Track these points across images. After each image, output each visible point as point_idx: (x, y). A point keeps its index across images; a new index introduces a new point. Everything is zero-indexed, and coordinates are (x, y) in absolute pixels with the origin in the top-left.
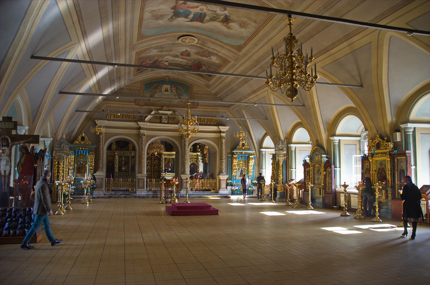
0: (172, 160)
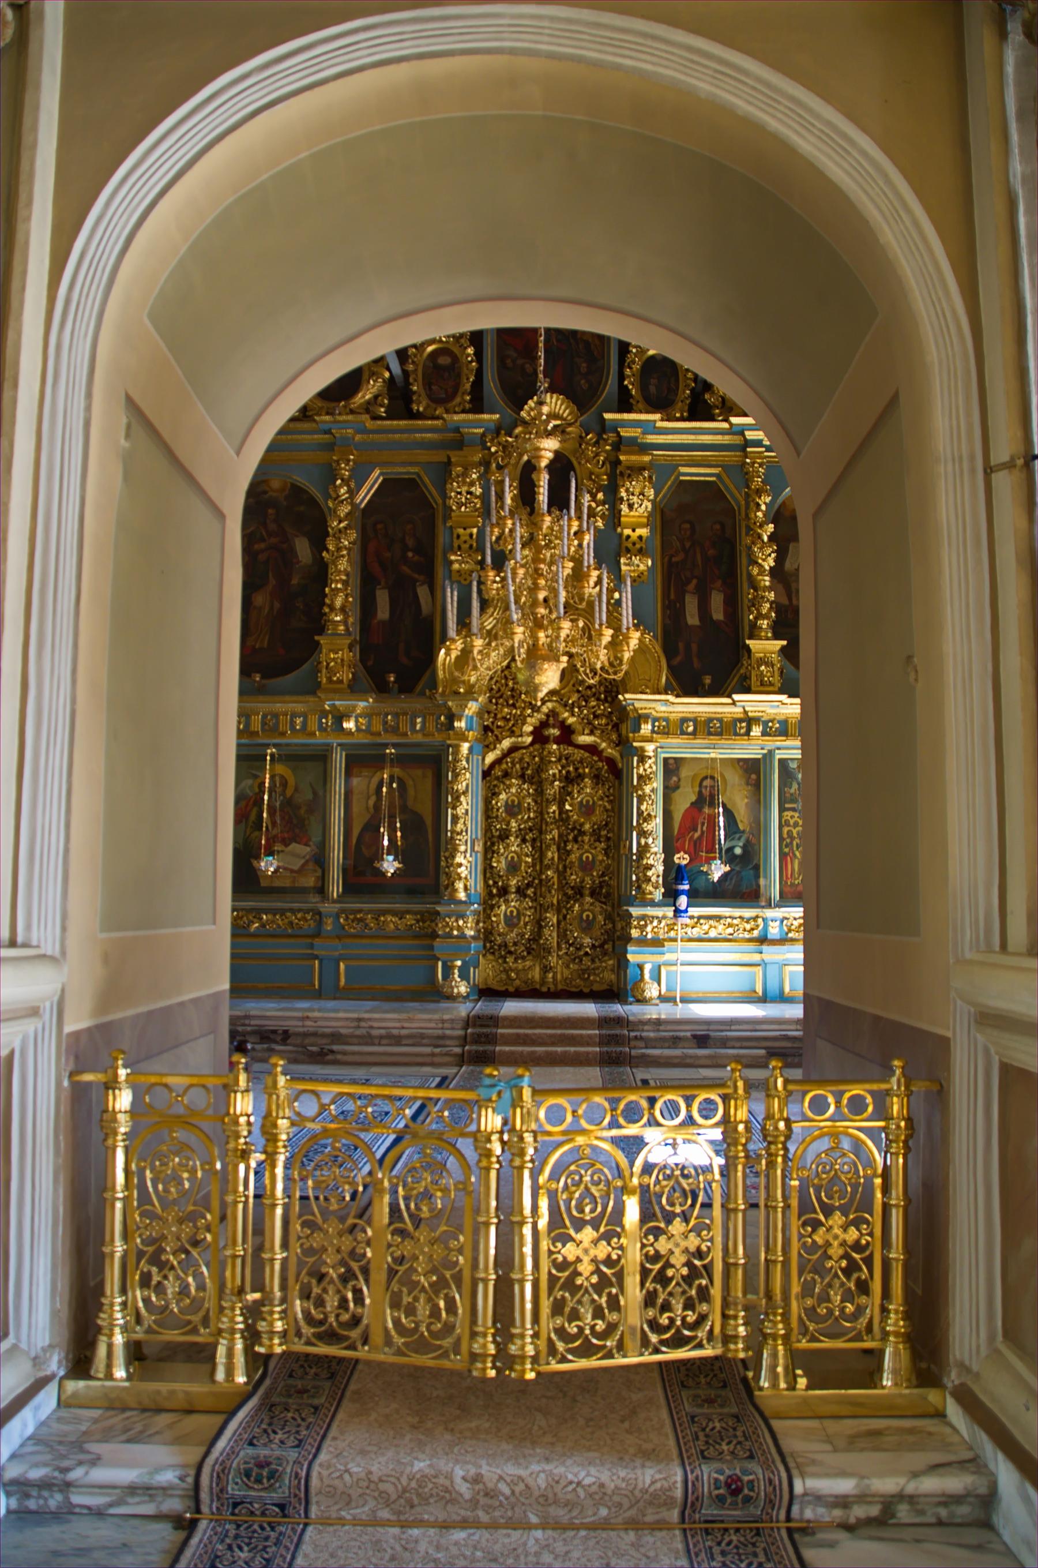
0: (734, 778)
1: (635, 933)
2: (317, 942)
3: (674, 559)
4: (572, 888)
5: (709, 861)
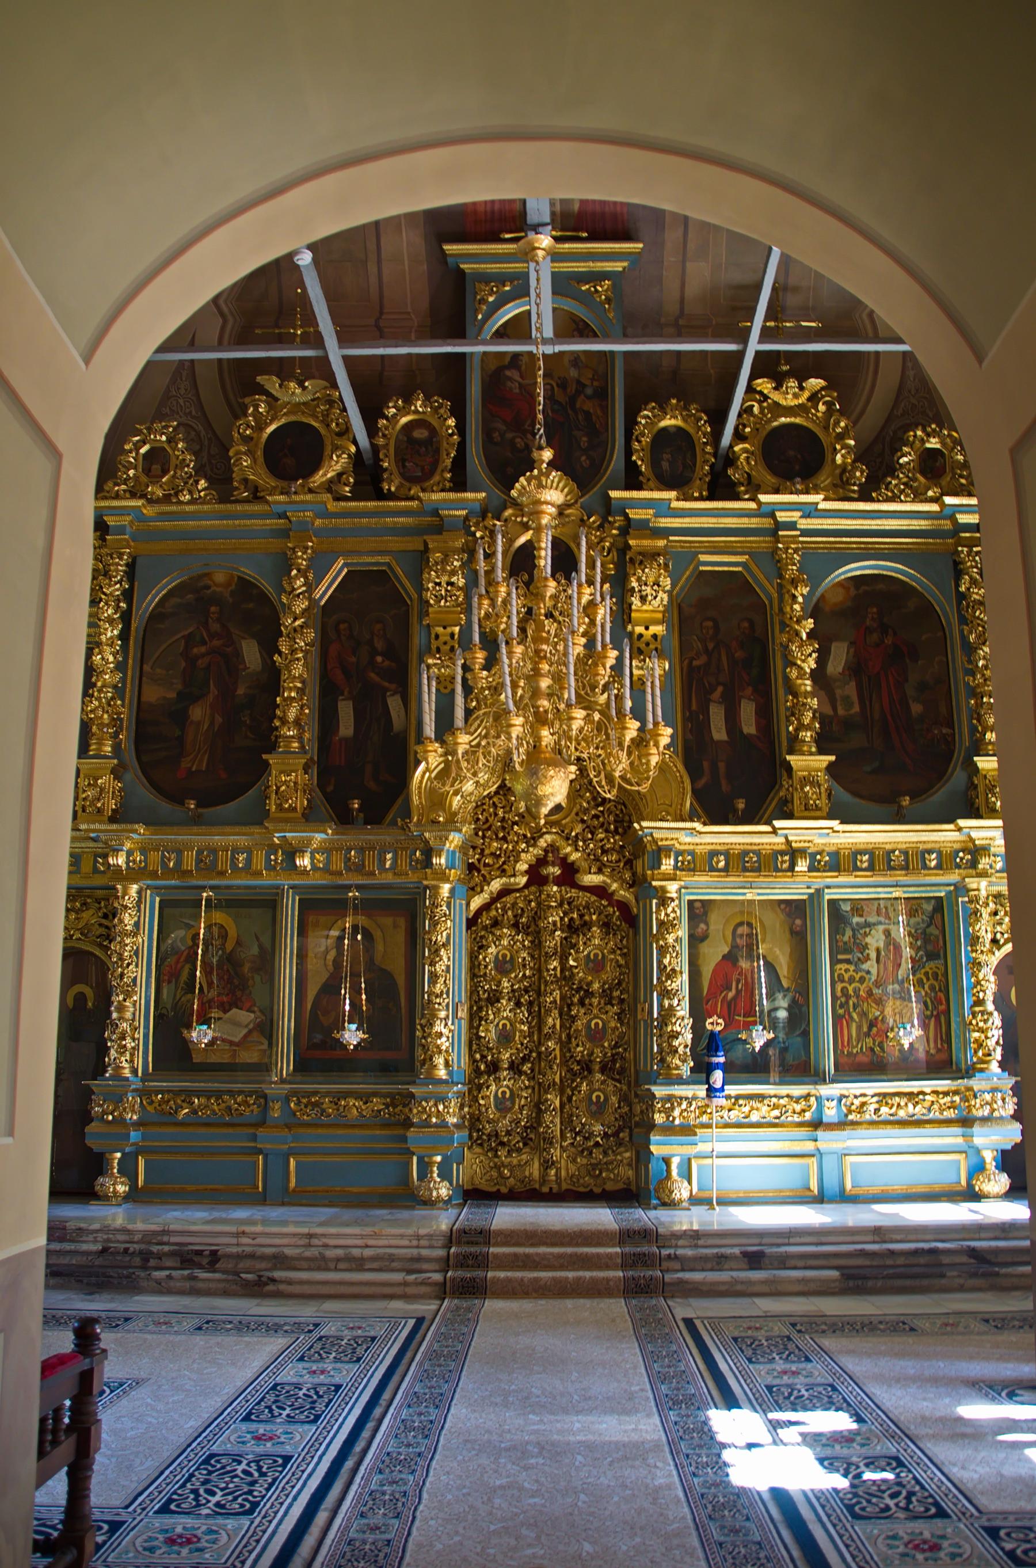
0: (775, 921)
1: (659, 1118)
2: (261, 1132)
3: (695, 663)
4: (578, 1062)
5: (748, 1026)
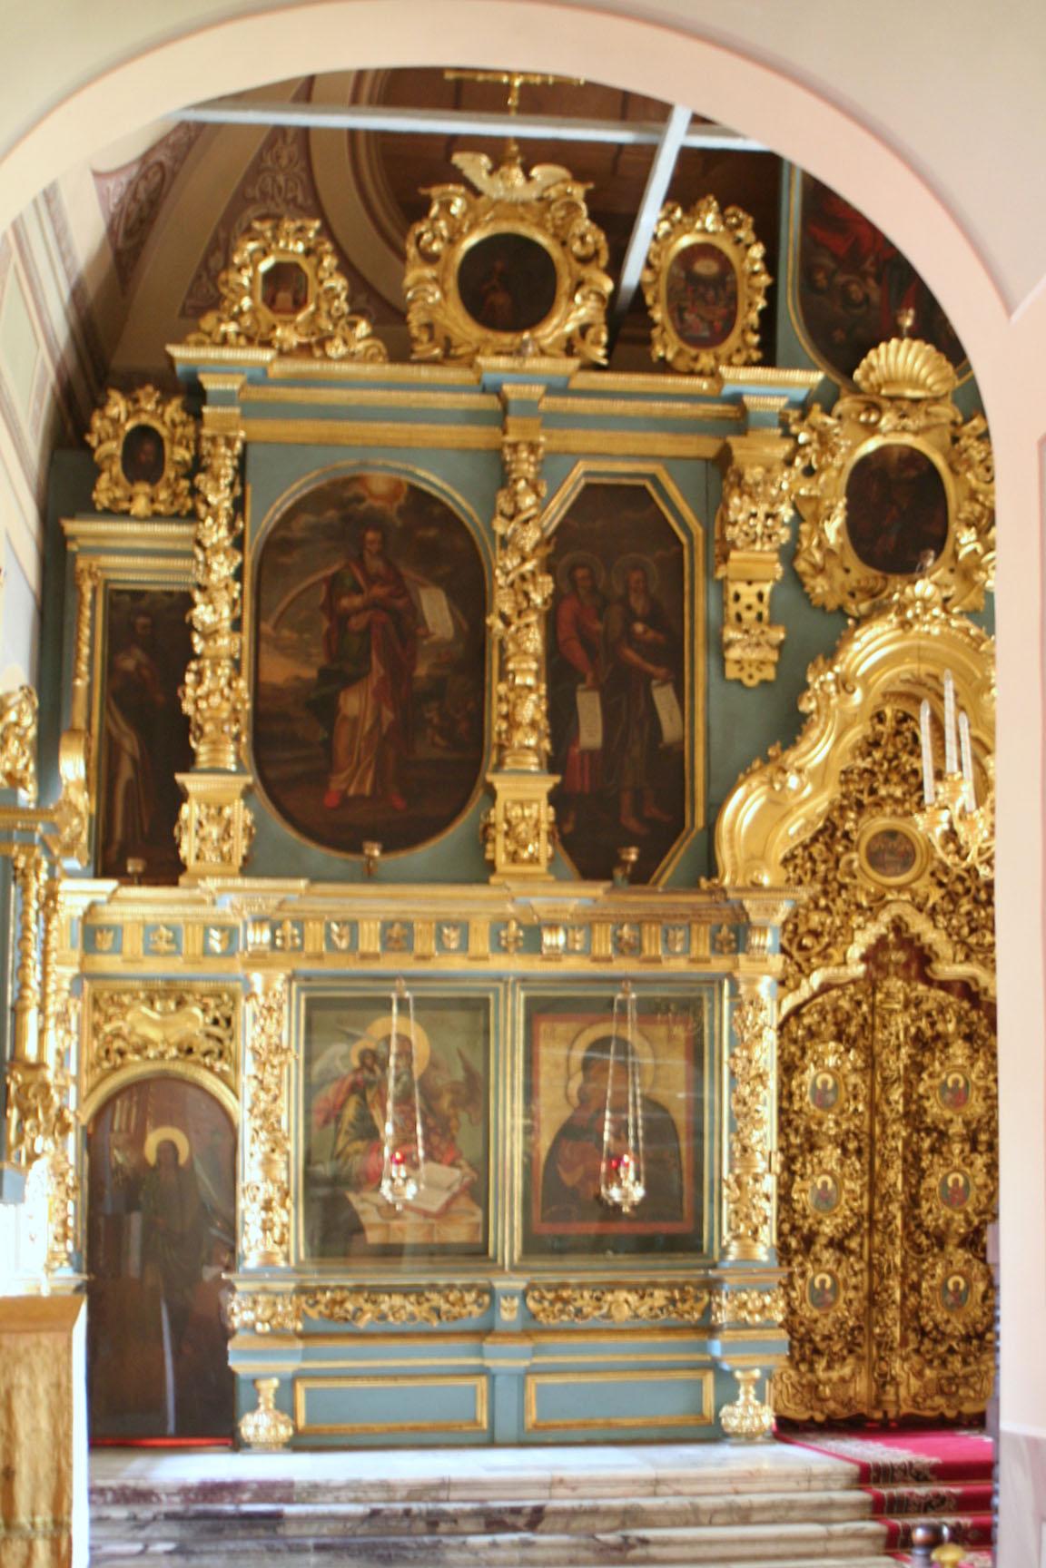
4: (927, 1235)
